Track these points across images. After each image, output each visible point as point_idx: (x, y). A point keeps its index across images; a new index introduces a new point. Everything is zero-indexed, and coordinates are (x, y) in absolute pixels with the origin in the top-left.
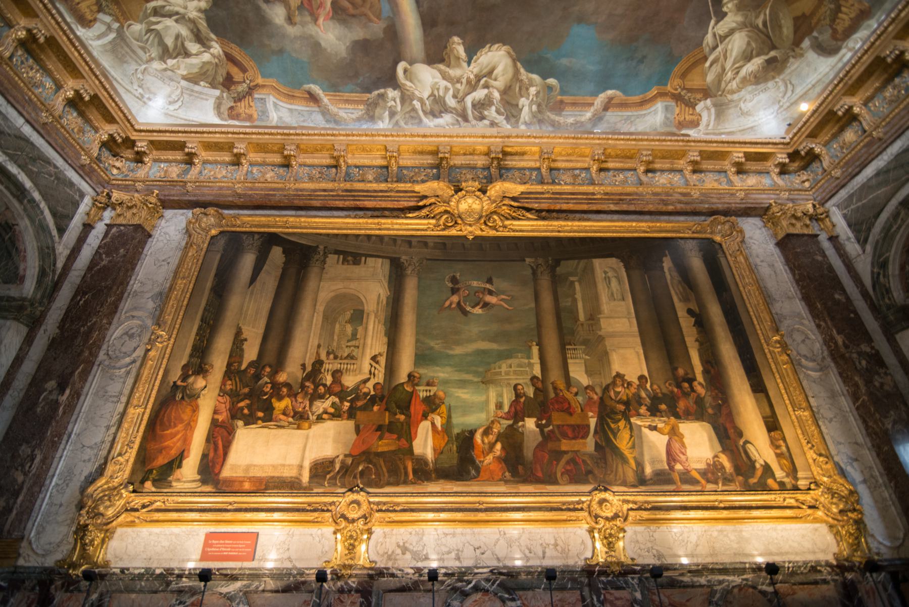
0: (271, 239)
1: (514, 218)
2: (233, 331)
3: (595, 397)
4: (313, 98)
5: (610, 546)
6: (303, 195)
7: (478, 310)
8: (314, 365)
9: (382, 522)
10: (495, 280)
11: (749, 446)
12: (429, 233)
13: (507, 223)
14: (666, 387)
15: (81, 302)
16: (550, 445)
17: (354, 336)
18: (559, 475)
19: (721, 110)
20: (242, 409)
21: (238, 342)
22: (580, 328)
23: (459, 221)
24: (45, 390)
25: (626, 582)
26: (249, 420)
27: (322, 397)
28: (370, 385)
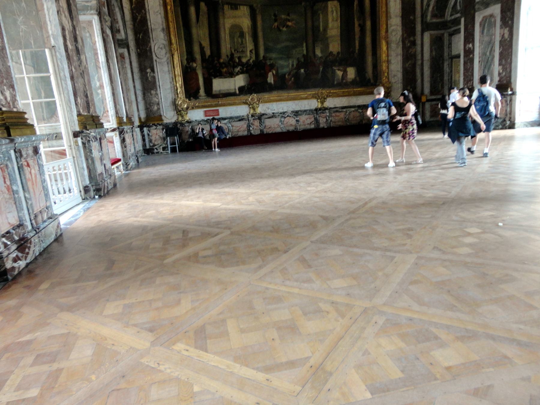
2: (199, 44)
7: (285, 29)
8: (231, 55)
15: (141, 37)
17: (242, 42)
21: (202, 48)
24: (148, 73)
26: (215, 77)
27: (236, 67)
28: (251, 61)
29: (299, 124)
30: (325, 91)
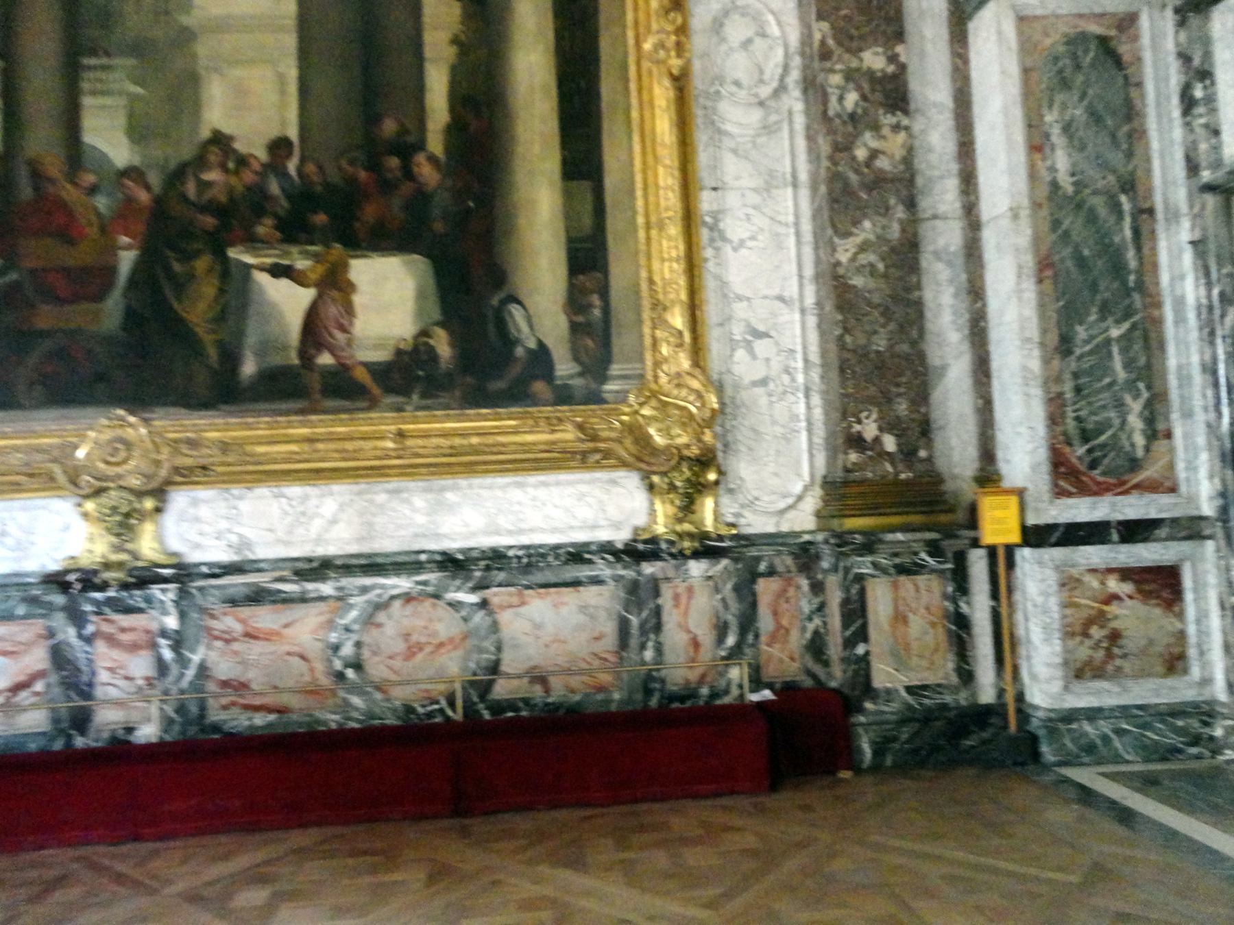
3: (143, 197)
11: (516, 311)
25: (149, 600)
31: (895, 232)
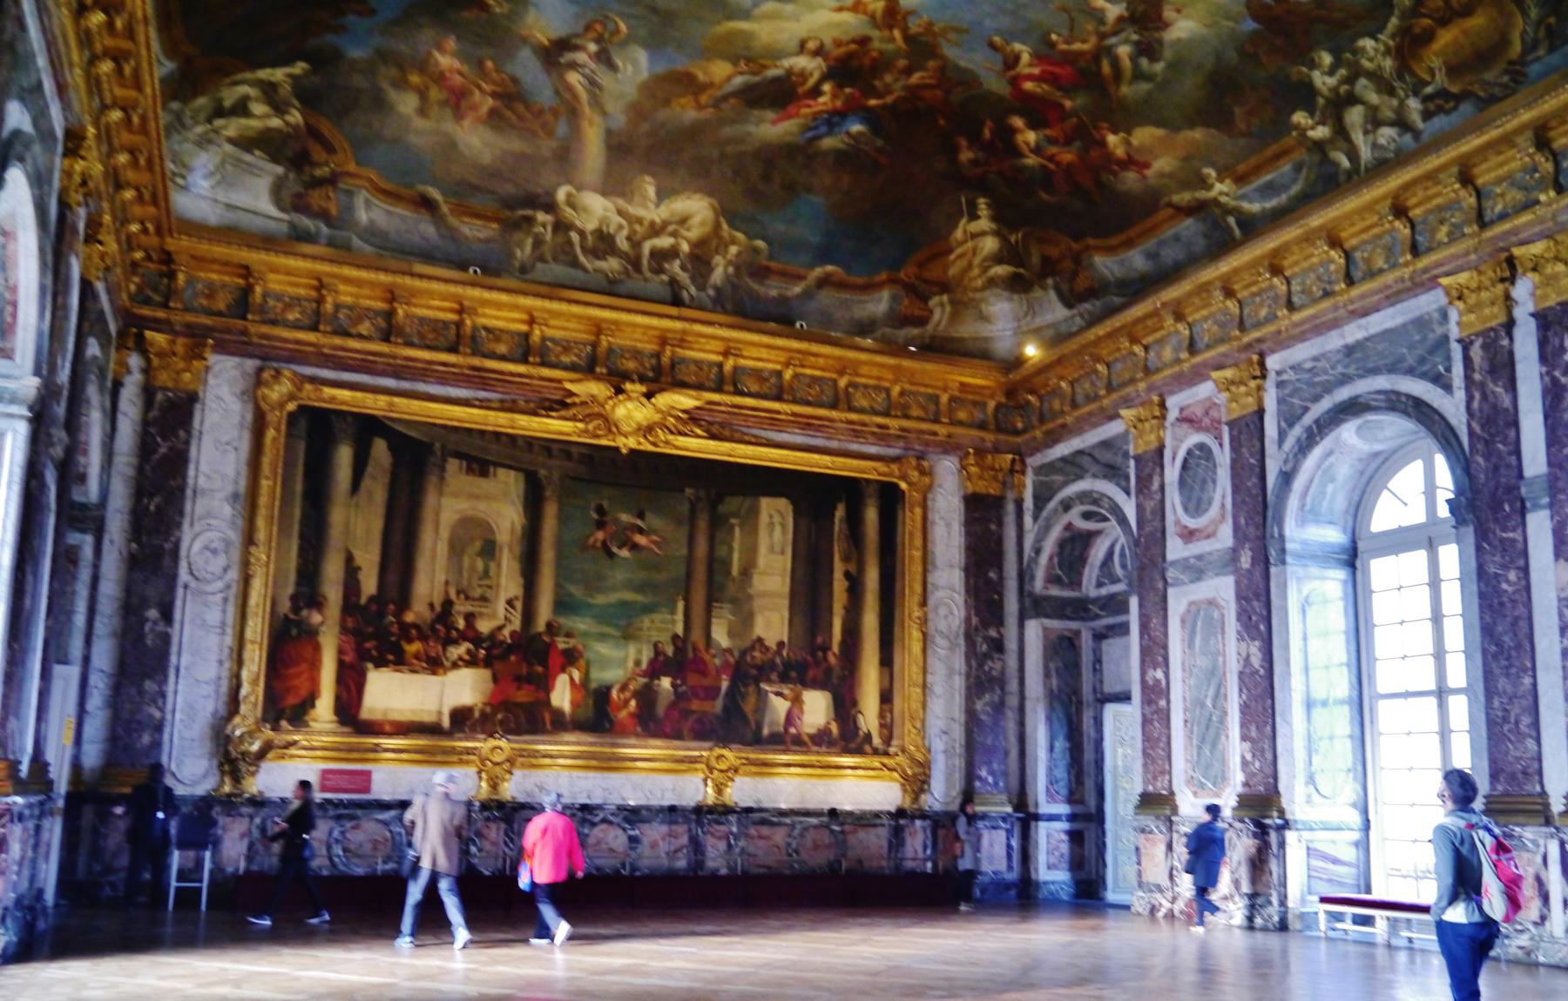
0: (367, 427)
1: (681, 434)
4: (426, 204)
5: (719, 790)
6: (415, 368)
7: (625, 553)
9: (523, 766)
10: (649, 515)
11: (860, 717)
12: (575, 439)
13: (671, 437)
14: (801, 655)
16: (682, 705)
17: (486, 574)
18: (685, 733)
19: (959, 308)
20: (369, 650)
21: (351, 572)
22: (731, 584)
23: (614, 429)
26: (380, 663)
27: (455, 642)
28: (506, 632)
29: (639, 851)
30: (731, 755)
31: (996, 699)
